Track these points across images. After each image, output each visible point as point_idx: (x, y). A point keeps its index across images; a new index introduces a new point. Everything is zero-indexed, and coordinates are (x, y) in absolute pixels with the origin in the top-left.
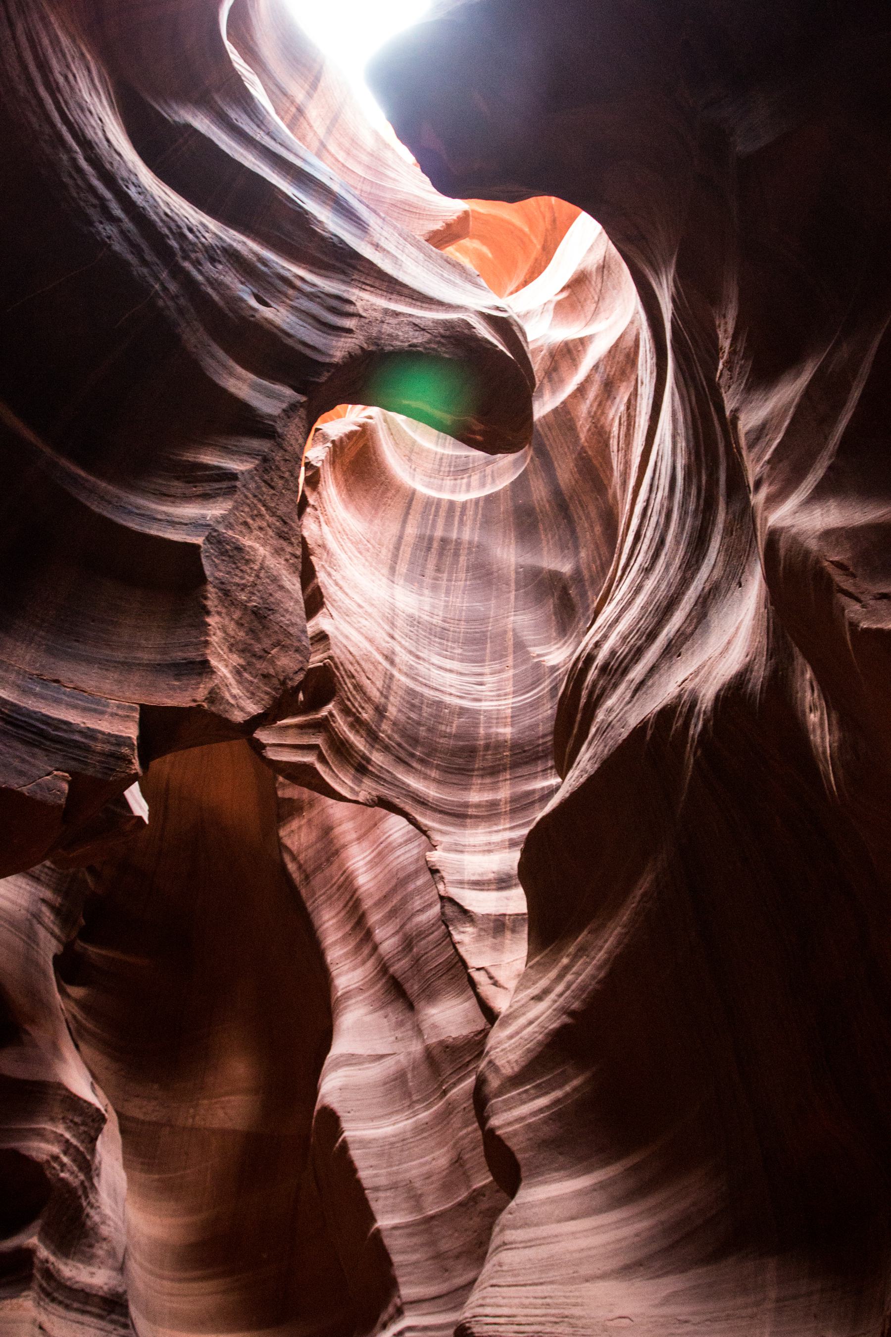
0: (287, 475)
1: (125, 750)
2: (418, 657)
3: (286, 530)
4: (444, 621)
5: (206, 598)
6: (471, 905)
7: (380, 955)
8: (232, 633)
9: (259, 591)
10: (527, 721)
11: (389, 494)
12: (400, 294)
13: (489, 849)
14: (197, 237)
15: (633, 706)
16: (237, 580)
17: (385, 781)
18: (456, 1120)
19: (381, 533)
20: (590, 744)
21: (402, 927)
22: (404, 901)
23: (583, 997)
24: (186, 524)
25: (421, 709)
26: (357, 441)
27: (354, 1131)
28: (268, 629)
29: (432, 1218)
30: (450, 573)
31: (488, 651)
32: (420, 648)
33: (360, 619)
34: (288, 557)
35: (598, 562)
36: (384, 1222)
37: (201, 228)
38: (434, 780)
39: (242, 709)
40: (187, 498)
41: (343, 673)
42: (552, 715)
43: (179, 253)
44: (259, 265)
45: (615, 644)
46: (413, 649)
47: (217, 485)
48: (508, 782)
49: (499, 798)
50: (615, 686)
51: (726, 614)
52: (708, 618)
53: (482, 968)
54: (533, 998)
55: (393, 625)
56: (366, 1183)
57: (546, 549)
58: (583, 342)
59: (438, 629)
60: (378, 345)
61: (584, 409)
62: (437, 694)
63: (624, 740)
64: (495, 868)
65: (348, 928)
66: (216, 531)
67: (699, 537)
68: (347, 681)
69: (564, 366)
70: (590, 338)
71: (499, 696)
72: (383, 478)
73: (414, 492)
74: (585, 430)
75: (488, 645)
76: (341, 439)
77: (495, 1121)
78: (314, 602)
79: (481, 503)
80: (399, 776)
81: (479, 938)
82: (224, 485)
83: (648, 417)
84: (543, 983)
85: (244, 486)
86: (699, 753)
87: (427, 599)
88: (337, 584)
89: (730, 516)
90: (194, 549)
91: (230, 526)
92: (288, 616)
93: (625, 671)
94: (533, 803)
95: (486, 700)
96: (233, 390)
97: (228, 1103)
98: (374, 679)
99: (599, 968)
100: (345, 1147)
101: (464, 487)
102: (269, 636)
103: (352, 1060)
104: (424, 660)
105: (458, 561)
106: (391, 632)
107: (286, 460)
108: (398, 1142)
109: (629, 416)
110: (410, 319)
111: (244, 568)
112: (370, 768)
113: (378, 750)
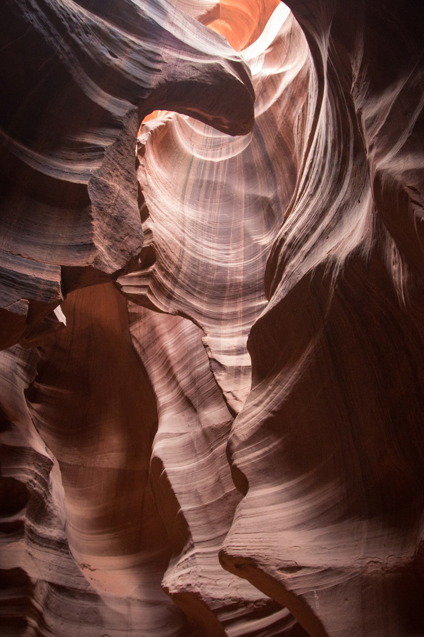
0: (129, 148)
1: (55, 288)
2: (196, 241)
3: (130, 177)
4: (209, 223)
5: (91, 212)
6: (224, 362)
7: (180, 387)
8: (105, 229)
9: (117, 208)
10: (251, 273)
11: (180, 159)
12: (185, 50)
13: (232, 336)
14: (78, 20)
15: (304, 264)
16: (106, 202)
17: (181, 302)
18: (218, 462)
19: (177, 179)
20: (283, 283)
21: (191, 373)
22: (191, 361)
23: (279, 404)
24: (79, 174)
25: (198, 267)
26: (163, 131)
27: (170, 468)
28: (122, 227)
29: (207, 506)
30: (212, 199)
31: (231, 238)
32: (198, 237)
33: (167, 223)
34: (131, 190)
35: (287, 192)
36: (184, 508)
37: (79, 14)
38: (205, 302)
39: (111, 267)
40: (79, 161)
41: (160, 249)
42: (263, 270)
43: (69, 29)
44: (111, 35)
45: (295, 233)
46: (194, 237)
47: (94, 154)
48: (242, 303)
49: (237, 310)
50: (295, 254)
51: (352, 217)
52: (343, 219)
53: (230, 392)
54: (254, 405)
55: (184, 225)
56: (176, 491)
57: (260, 186)
58: (280, 76)
59: (206, 227)
60: (174, 78)
61: (280, 112)
62: (206, 259)
63: (300, 281)
64: (236, 344)
65: (164, 374)
66: (95, 177)
67: (339, 178)
68: (162, 253)
69: (269, 91)
70: (283, 73)
71: (236, 260)
72: (177, 150)
73: (193, 157)
74: (280, 123)
75: (231, 235)
76: (155, 130)
77: (236, 462)
78: (145, 214)
79: (227, 163)
80: (188, 300)
81: (228, 378)
82: (98, 153)
83: (313, 115)
84: (260, 398)
85: (108, 154)
86: (337, 286)
87: (200, 212)
88: (155, 205)
89: (355, 166)
90: (84, 187)
91: (102, 175)
92: (132, 220)
93: (300, 247)
94: (254, 313)
95: (230, 263)
96: (100, 103)
97: (110, 455)
98: (175, 252)
99: (287, 390)
100: (165, 475)
101: (218, 154)
102: (123, 231)
103: (168, 436)
104: (199, 243)
105: (215, 193)
106: (183, 229)
107: (128, 140)
108: (190, 473)
109: (303, 115)
110: (191, 64)
111: (109, 196)
112: (174, 296)
113: (177, 288)
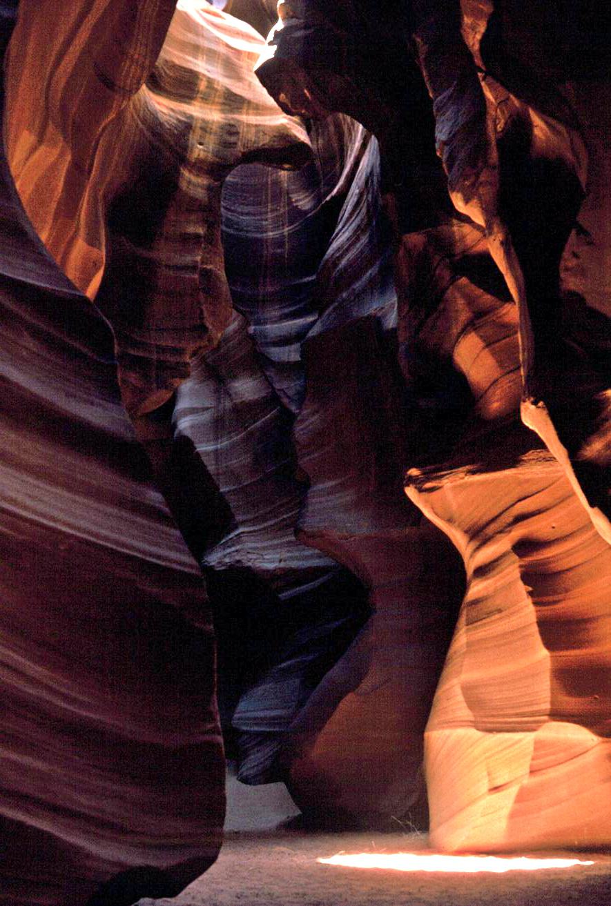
103: (193, 411)
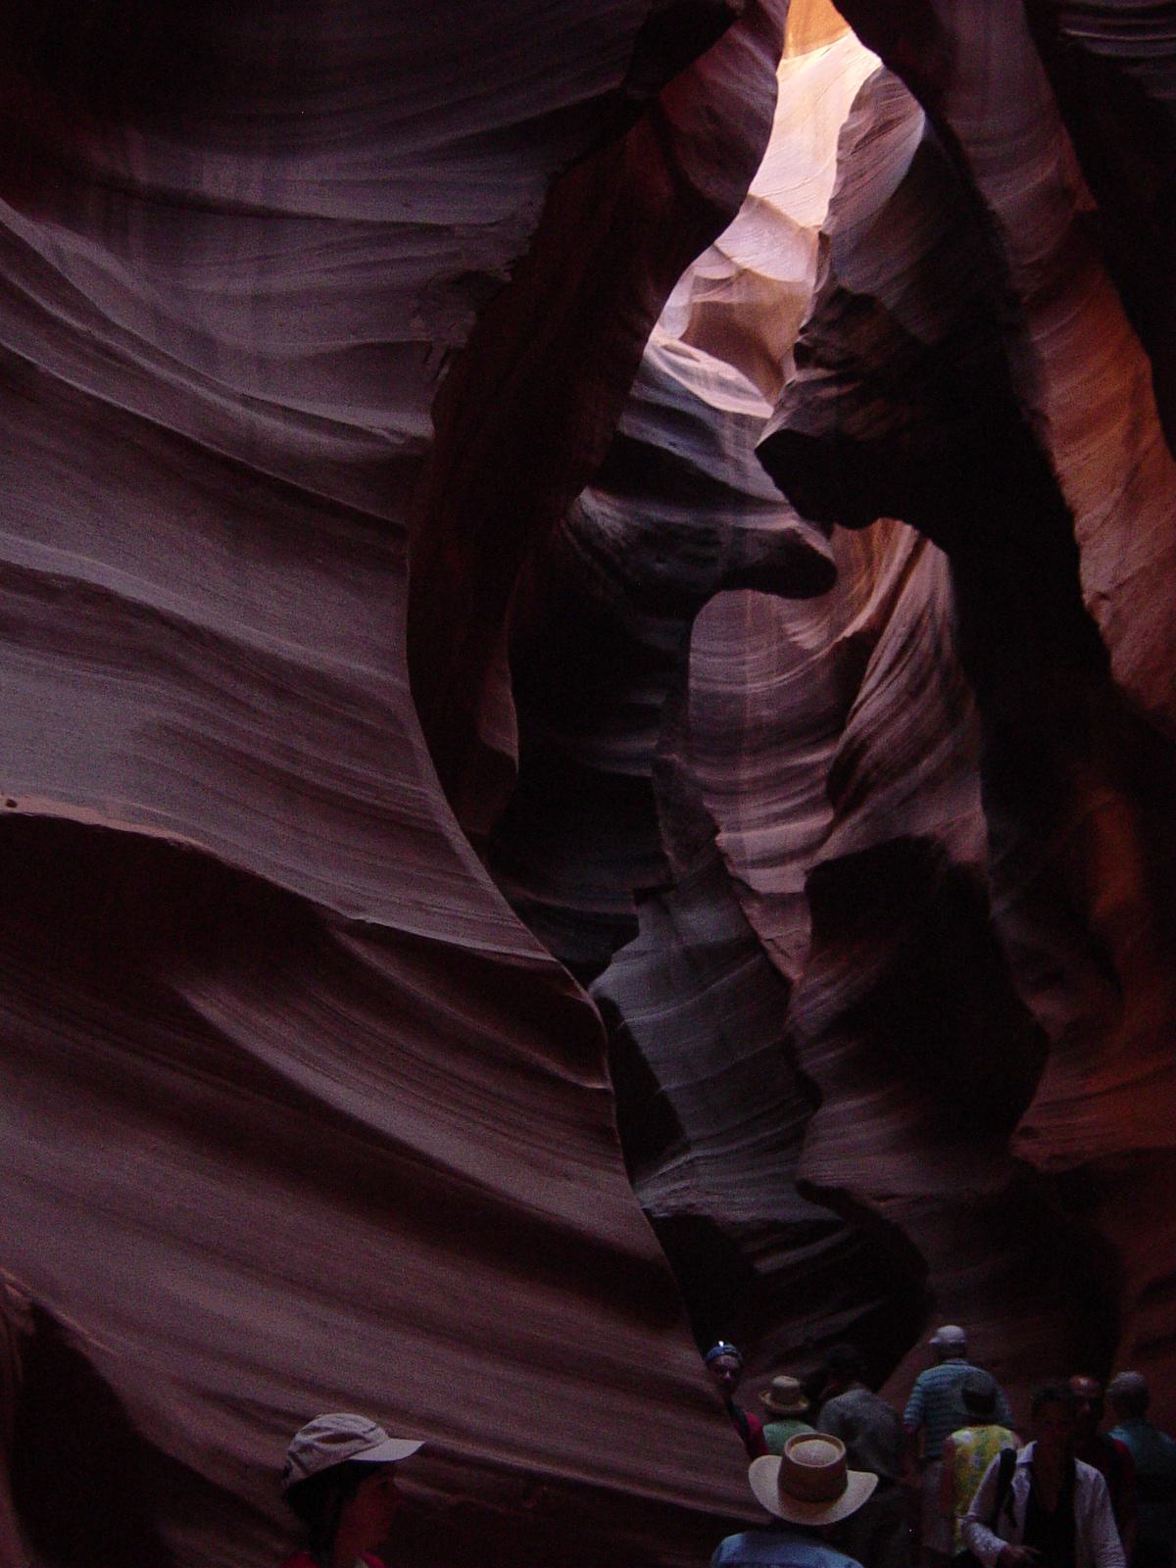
54: (822, 985)
56: (649, 1058)
90: (643, 781)
